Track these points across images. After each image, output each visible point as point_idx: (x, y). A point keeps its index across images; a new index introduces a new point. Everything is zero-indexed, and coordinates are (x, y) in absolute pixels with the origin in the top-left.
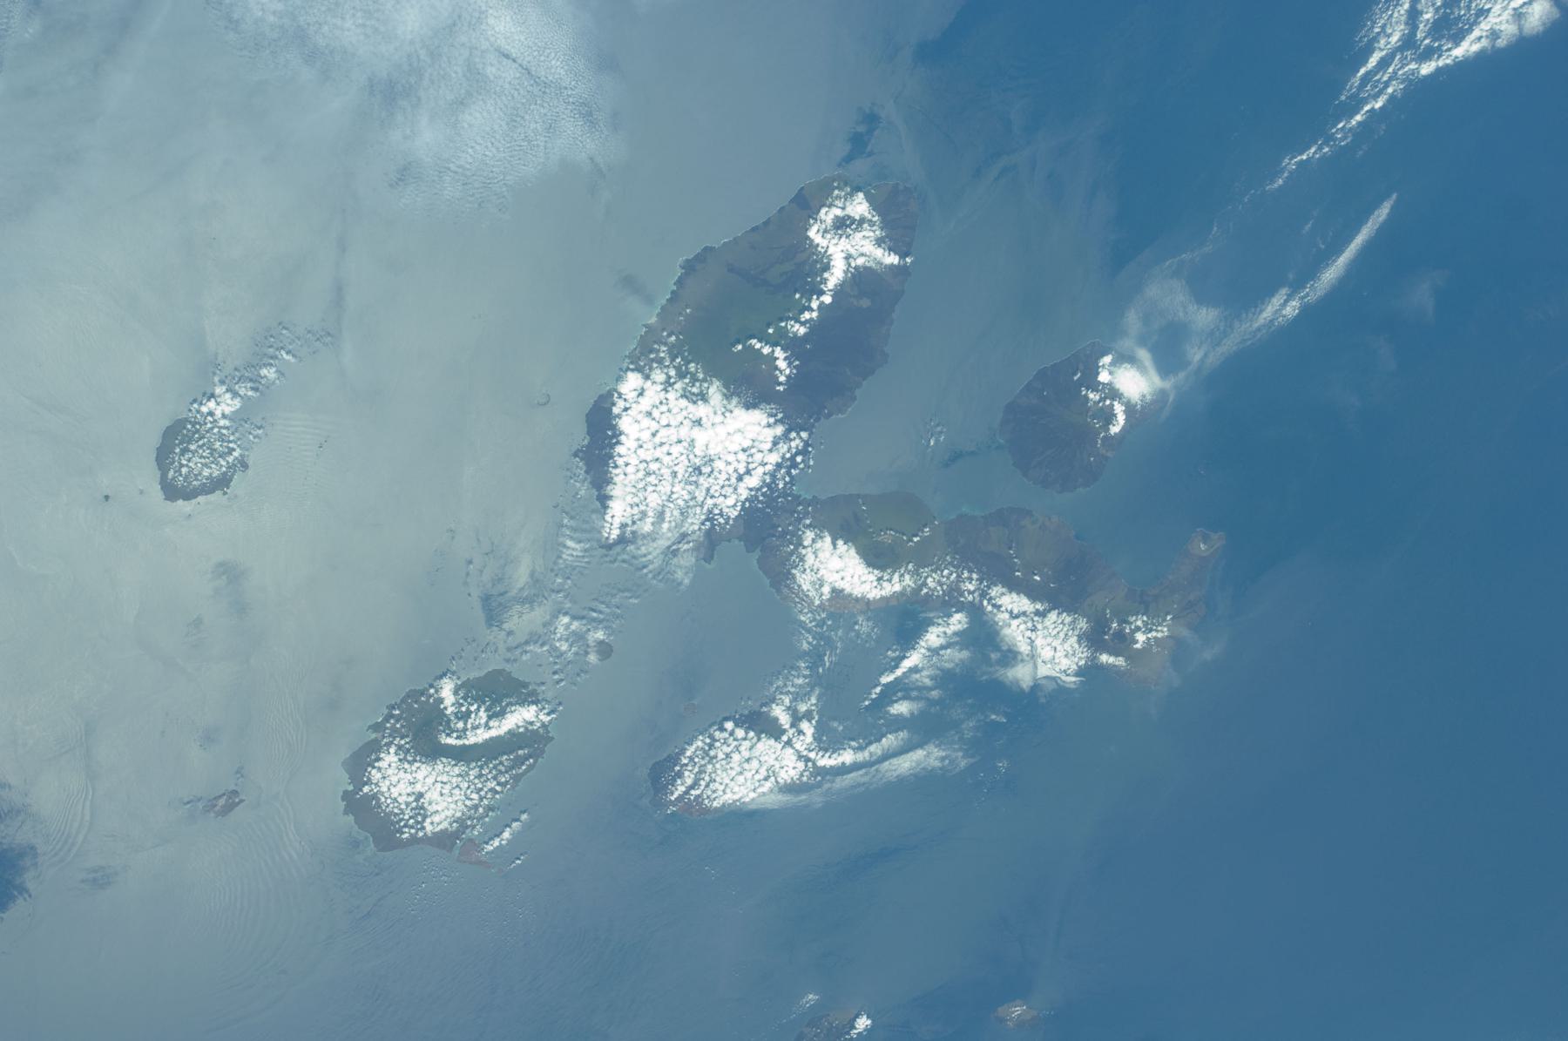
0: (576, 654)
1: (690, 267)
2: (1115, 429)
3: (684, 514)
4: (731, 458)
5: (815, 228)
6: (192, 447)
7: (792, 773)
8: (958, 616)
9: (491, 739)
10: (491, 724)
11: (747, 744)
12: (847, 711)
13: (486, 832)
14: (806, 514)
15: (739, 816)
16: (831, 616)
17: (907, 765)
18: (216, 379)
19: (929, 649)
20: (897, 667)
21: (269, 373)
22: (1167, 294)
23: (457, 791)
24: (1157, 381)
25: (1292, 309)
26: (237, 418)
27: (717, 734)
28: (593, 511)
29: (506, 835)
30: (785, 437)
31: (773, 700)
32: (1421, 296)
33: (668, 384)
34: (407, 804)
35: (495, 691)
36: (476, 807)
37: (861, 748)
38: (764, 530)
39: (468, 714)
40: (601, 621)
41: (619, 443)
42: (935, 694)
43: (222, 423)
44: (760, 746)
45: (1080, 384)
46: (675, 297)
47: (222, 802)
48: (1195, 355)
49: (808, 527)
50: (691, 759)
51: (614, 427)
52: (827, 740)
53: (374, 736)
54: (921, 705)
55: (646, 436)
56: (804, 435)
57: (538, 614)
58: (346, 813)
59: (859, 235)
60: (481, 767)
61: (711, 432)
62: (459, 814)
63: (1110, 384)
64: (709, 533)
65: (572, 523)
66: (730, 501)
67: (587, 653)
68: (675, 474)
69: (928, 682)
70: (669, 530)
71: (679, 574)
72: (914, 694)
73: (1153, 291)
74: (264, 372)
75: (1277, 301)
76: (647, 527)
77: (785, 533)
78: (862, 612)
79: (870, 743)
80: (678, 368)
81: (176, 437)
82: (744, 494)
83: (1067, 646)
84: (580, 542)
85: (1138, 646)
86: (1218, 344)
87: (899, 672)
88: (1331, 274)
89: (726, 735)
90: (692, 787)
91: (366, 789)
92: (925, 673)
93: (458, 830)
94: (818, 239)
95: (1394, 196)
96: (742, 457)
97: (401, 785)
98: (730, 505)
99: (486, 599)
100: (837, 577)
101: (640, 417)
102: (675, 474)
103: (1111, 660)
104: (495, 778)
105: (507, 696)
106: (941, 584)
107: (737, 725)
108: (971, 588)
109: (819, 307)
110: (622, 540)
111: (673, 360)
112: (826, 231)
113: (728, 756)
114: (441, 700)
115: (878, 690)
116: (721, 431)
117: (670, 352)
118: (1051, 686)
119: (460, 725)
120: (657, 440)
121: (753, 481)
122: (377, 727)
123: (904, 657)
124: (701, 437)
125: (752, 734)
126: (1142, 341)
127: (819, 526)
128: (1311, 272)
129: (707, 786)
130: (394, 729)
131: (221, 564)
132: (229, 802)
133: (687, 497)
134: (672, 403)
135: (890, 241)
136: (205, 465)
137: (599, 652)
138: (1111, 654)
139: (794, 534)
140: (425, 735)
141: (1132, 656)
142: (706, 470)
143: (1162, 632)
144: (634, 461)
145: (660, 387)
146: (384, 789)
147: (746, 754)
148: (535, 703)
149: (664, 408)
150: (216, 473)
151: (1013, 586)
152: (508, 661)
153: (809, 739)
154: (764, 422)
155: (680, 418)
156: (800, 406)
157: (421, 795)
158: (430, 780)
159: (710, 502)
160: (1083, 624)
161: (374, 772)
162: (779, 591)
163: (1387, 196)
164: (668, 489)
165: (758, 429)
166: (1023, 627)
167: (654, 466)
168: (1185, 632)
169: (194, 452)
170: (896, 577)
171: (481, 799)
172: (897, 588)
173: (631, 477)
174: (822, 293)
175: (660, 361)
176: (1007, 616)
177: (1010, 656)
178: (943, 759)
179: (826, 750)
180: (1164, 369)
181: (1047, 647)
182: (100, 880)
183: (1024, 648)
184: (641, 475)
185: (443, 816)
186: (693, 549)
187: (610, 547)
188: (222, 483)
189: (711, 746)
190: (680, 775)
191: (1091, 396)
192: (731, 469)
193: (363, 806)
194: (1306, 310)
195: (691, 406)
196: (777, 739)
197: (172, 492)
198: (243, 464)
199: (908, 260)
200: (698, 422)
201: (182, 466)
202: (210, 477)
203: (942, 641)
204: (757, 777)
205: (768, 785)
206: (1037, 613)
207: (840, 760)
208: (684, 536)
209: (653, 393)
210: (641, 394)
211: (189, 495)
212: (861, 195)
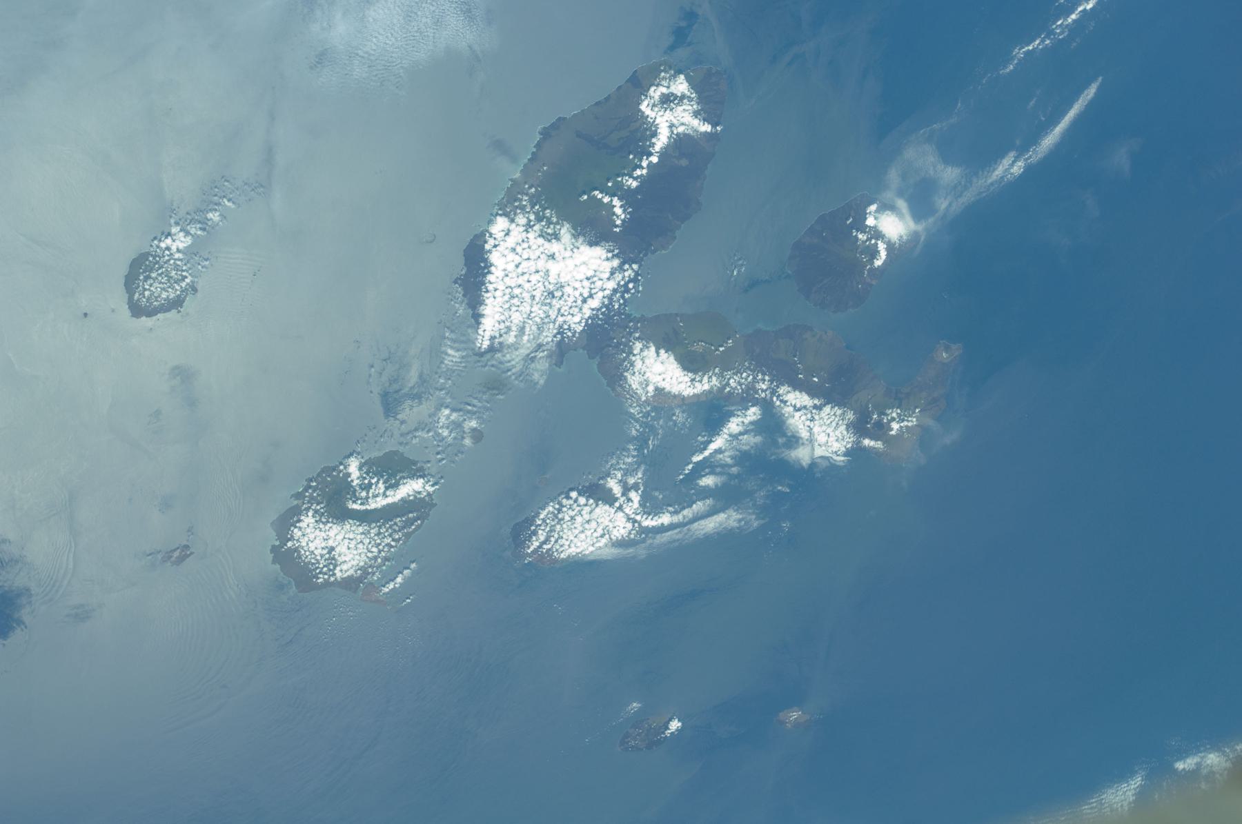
0: (455, 438)
1: (546, 134)
2: (878, 263)
3: (540, 328)
4: (578, 285)
5: (646, 103)
6: (153, 275)
7: (623, 531)
8: (753, 409)
9: (388, 505)
10: (388, 493)
11: (587, 509)
12: (666, 483)
13: (383, 577)
14: (636, 329)
15: (580, 566)
16: (655, 409)
17: (712, 525)
18: (172, 221)
19: (730, 435)
20: (705, 449)
21: (214, 216)
22: (921, 157)
23: (360, 546)
24: (912, 225)
25: (1018, 169)
26: (189, 252)
27: (565, 502)
28: (469, 327)
29: (399, 580)
30: (621, 268)
31: (608, 475)
32: (1120, 158)
33: (528, 227)
34: (322, 556)
35: (391, 468)
36: (375, 558)
37: (676, 512)
38: (605, 340)
39: (370, 486)
40: (475, 413)
41: (489, 272)
42: (734, 470)
43: (177, 256)
44: (598, 510)
45: (852, 227)
47: (176, 554)
48: (942, 204)
49: (637, 339)
50: (544, 520)
51: (486, 260)
52: (650, 506)
53: (296, 502)
54: (724, 478)
55: (511, 267)
56: (635, 267)
57: (424, 409)
58: (274, 562)
59: (680, 108)
60: (380, 527)
61: (562, 264)
62: (362, 564)
63: (875, 227)
64: (559, 344)
65: (453, 336)
66: (577, 319)
67: (463, 438)
68: (533, 297)
69: (729, 460)
71: (536, 376)
72: (718, 470)
73: (910, 153)
74: (210, 215)
75: (1006, 162)
76: (511, 339)
77: (619, 344)
78: (680, 406)
79: (684, 508)
80: (536, 214)
81: (141, 266)
82: (588, 313)
83: (837, 433)
85: (893, 433)
86: (960, 196)
87: (707, 453)
88: (1049, 141)
89: (571, 502)
90: (544, 543)
91: (289, 544)
92: (727, 454)
93: (361, 576)
94: (648, 112)
95: (1100, 79)
96: (586, 283)
97: (317, 541)
98: (576, 322)
99: (385, 395)
100: (659, 378)
101: (506, 252)
102: (533, 297)
103: (872, 443)
104: (390, 535)
105: (400, 471)
106: (741, 384)
107: (580, 494)
108: (764, 387)
109: (648, 166)
110: (491, 349)
111: (533, 207)
112: (654, 105)
113: (572, 518)
114: (349, 475)
115: (690, 467)
116: (570, 263)
117: (530, 201)
118: (825, 464)
119: (364, 494)
120: (520, 270)
121: (594, 303)
122: (299, 496)
123: (711, 441)
124: (554, 268)
125: (591, 501)
126: (900, 194)
127: (646, 338)
128: (1033, 139)
129: (556, 541)
130: (311, 497)
131: (177, 367)
132: (184, 553)
133: (543, 316)
135: (704, 113)
136: (163, 289)
137: (472, 437)
138: (872, 439)
139: (626, 345)
140: (336, 502)
141: (888, 440)
142: (558, 294)
143: (912, 422)
144: (501, 287)
145: (522, 229)
146: (304, 544)
147: (587, 517)
148: (422, 477)
149: (525, 245)
150: (172, 296)
151: (797, 386)
152: (401, 444)
153: (636, 505)
154: (604, 256)
155: (538, 253)
156: (631, 244)
157: (332, 549)
158: (340, 537)
159: (561, 319)
160: (850, 416)
161: (296, 530)
162: (614, 389)
163: (1094, 79)
164: (528, 308)
165: (599, 261)
166: (804, 418)
167: (517, 291)
168: (930, 422)
169: (155, 279)
170: (706, 379)
171: (380, 552)
172: (706, 387)
173: (499, 300)
174: (650, 154)
175: (523, 208)
176: (791, 409)
177: (794, 441)
178: (740, 521)
179: (649, 514)
180: (917, 215)
181: (822, 433)
182: (81, 615)
183: (804, 434)
184: (506, 298)
185: (350, 565)
186: (548, 357)
187: (482, 355)
188: (177, 303)
189: (559, 511)
190: (535, 533)
191: (860, 236)
192: (577, 294)
193: (287, 558)
194: (1029, 169)
195: (546, 244)
196: (611, 505)
197: (137, 310)
198: (193, 288)
199: (719, 128)
200: (552, 257)
201: (145, 290)
202: (167, 299)
203: (740, 428)
204: (595, 535)
205: (604, 541)
206: (815, 407)
207: (660, 521)
208: (540, 346)
209: (517, 233)
210: (507, 234)
211: (151, 313)
212: (682, 77)
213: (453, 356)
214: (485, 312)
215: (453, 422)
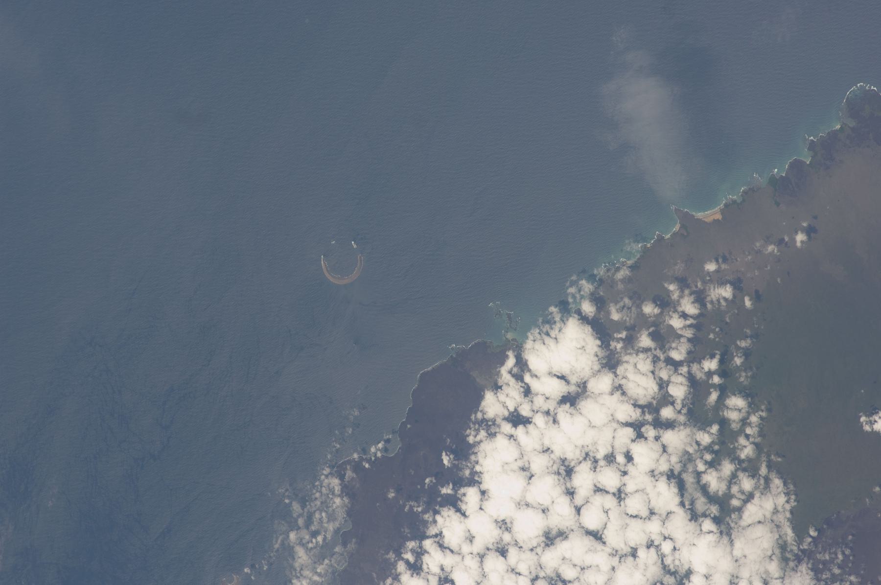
33: (649, 418)
41: (454, 502)
46: (789, 188)
51: (464, 451)
55: (529, 527)
101: (539, 463)
111: (694, 357)
117: (699, 324)
134: (637, 479)
145: (627, 412)
149: (609, 478)
175: (663, 337)
195: (680, 519)
210: (570, 400)
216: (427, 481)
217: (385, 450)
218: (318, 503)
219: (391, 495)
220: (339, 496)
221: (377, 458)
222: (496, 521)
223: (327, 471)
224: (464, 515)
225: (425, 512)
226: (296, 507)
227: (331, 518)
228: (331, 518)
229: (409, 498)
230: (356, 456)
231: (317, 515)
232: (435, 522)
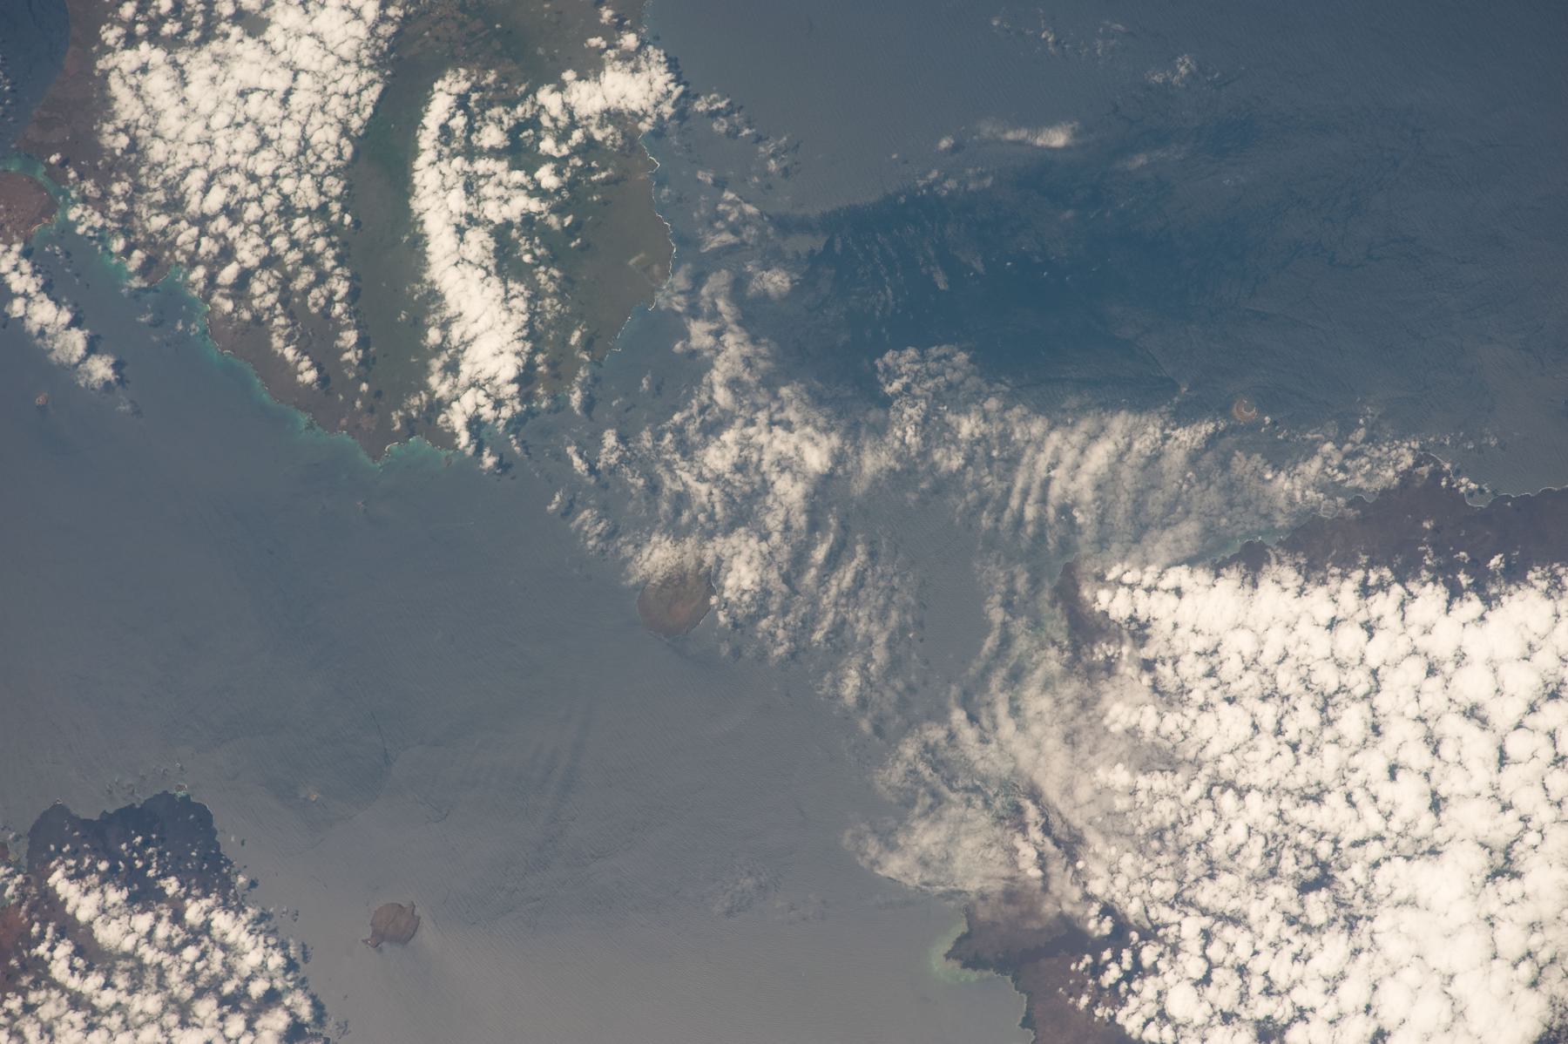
0: (682, 499)
9: (419, 242)
23: (247, 138)
28: (1208, 531)
35: (586, 251)
36: (174, 205)
41: (1455, 592)
55: (1472, 684)
61: (1463, 911)
62: (158, 151)
64: (1071, 937)
70: (1105, 790)
71: (926, 837)
84: (1099, 487)
110: (1087, 628)
119: (491, 136)
120: (1452, 725)
124: (1447, 883)
142: (1317, 907)
144: (1377, 651)
167: (1352, 720)
171: (202, 221)
173: (1321, 643)
184: (1327, 678)
187: (1068, 594)
190: (144, 896)
208: (1071, 845)
213: (1079, 459)
214: (1267, 587)
215: (766, 487)
216: (1463, 554)
217: (1471, 493)
218: (1377, 454)
219: (1427, 525)
220: (1397, 472)
221: (1457, 489)
222: (1460, 648)
223: (1415, 445)
224: (1448, 610)
225: (1428, 568)
226: (1360, 434)
227: (1369, 476)
228: (1369, 476)
229: (1434, 545)
230: (1447, 466)
231: (1364, 460)
232: (1424, 584)
